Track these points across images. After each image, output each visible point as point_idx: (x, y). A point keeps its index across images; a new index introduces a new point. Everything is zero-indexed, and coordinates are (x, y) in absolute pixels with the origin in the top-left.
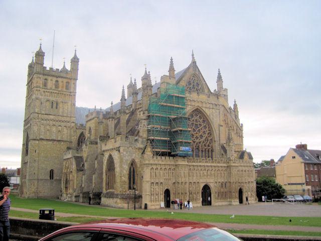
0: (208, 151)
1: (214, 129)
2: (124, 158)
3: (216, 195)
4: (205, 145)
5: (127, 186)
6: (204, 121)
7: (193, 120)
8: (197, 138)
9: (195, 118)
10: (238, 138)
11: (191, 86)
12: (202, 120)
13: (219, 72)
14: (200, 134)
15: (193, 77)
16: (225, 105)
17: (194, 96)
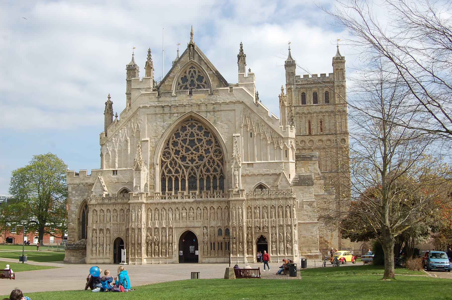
0: (215, 178)
1: (221, 143)
2: (73, 199)
3: (206, 247)
4: (208, 170)
5: (76, 235)
6: (207, 134)
7: (186, 135)
8: (192, 160)
9: (189, 130)
10: (278, 150)
11: (188, 83)
12: (203, 132)
13: (241, 47)
14: (200, 153)
15: (192, 67)
16: (246, 101)
17: (184, 98)
